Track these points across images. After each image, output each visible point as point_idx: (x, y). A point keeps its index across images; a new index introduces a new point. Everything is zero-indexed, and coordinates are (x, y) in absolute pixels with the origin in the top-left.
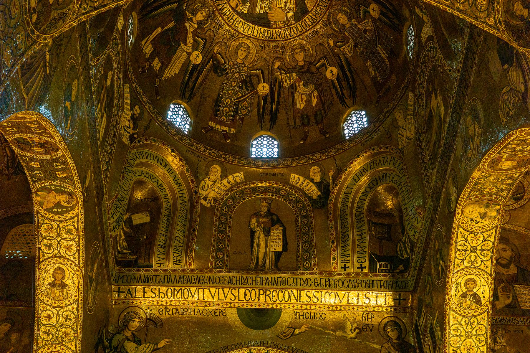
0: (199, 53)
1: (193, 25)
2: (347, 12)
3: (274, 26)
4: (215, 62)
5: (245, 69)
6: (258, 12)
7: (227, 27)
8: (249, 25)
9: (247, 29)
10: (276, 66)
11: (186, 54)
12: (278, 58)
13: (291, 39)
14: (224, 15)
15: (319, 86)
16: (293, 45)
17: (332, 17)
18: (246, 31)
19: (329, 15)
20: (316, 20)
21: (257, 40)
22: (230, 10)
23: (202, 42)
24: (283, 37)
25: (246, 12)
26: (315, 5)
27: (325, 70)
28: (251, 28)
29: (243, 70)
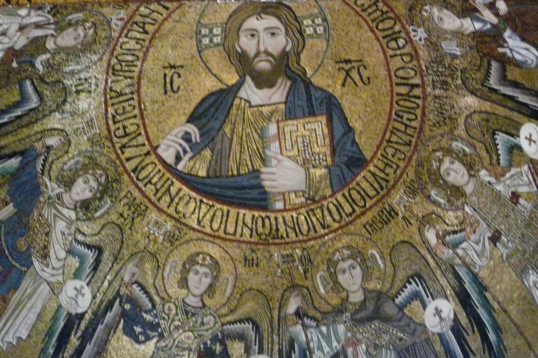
0: (84, 284)
1: (65, 211)
2: (465, 155)
3: (279, 205)
4: (127, 307)
5: (209, 320)
6: (235, 173)
7: (153, 215)
8: (213, 206)
9: (208, 217)
10: (291, 308)
11: (48, 288)
12: (294, 286)
13: (327, 234)
14: (145, 185)
15: (408, 352)
16: (331, 251)
17: (429, 170)
18: (206, 222)
19: (420, 164)
20: (387, 181)
21: (235, 244)
22: (160, 170)
23: (91, 256)
24: (305, 233)
25: (202, 173)
26: (381, 142)
27: (421, 309)
28: (219, 213)
29: (203, 324)
